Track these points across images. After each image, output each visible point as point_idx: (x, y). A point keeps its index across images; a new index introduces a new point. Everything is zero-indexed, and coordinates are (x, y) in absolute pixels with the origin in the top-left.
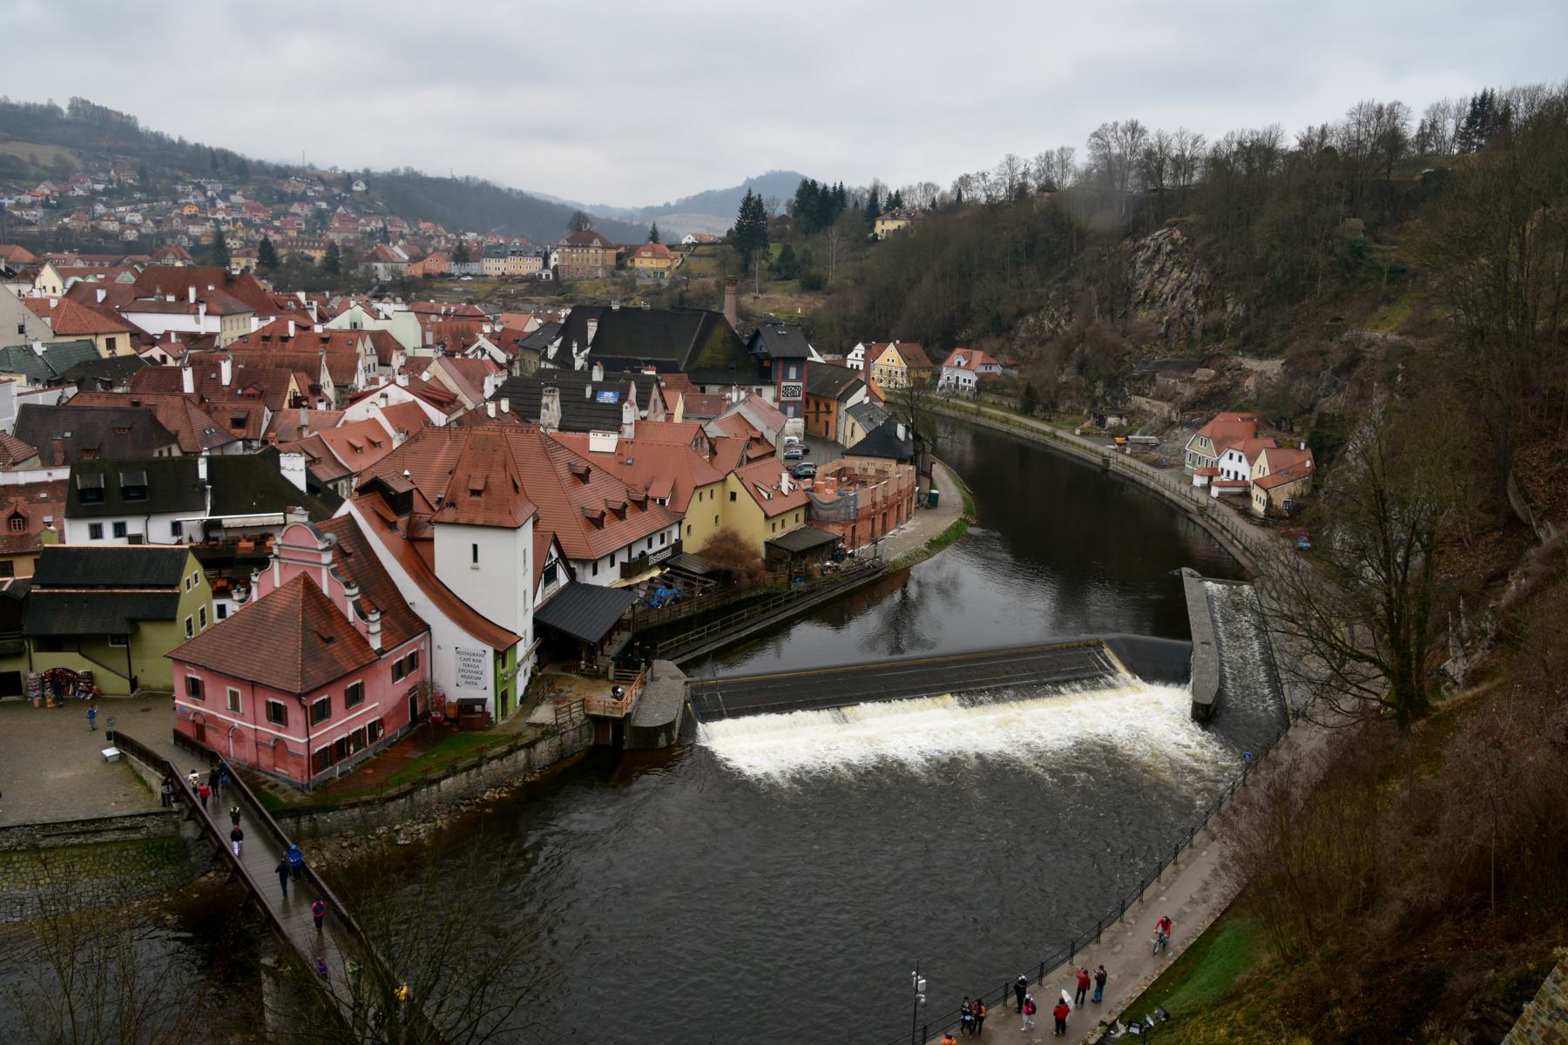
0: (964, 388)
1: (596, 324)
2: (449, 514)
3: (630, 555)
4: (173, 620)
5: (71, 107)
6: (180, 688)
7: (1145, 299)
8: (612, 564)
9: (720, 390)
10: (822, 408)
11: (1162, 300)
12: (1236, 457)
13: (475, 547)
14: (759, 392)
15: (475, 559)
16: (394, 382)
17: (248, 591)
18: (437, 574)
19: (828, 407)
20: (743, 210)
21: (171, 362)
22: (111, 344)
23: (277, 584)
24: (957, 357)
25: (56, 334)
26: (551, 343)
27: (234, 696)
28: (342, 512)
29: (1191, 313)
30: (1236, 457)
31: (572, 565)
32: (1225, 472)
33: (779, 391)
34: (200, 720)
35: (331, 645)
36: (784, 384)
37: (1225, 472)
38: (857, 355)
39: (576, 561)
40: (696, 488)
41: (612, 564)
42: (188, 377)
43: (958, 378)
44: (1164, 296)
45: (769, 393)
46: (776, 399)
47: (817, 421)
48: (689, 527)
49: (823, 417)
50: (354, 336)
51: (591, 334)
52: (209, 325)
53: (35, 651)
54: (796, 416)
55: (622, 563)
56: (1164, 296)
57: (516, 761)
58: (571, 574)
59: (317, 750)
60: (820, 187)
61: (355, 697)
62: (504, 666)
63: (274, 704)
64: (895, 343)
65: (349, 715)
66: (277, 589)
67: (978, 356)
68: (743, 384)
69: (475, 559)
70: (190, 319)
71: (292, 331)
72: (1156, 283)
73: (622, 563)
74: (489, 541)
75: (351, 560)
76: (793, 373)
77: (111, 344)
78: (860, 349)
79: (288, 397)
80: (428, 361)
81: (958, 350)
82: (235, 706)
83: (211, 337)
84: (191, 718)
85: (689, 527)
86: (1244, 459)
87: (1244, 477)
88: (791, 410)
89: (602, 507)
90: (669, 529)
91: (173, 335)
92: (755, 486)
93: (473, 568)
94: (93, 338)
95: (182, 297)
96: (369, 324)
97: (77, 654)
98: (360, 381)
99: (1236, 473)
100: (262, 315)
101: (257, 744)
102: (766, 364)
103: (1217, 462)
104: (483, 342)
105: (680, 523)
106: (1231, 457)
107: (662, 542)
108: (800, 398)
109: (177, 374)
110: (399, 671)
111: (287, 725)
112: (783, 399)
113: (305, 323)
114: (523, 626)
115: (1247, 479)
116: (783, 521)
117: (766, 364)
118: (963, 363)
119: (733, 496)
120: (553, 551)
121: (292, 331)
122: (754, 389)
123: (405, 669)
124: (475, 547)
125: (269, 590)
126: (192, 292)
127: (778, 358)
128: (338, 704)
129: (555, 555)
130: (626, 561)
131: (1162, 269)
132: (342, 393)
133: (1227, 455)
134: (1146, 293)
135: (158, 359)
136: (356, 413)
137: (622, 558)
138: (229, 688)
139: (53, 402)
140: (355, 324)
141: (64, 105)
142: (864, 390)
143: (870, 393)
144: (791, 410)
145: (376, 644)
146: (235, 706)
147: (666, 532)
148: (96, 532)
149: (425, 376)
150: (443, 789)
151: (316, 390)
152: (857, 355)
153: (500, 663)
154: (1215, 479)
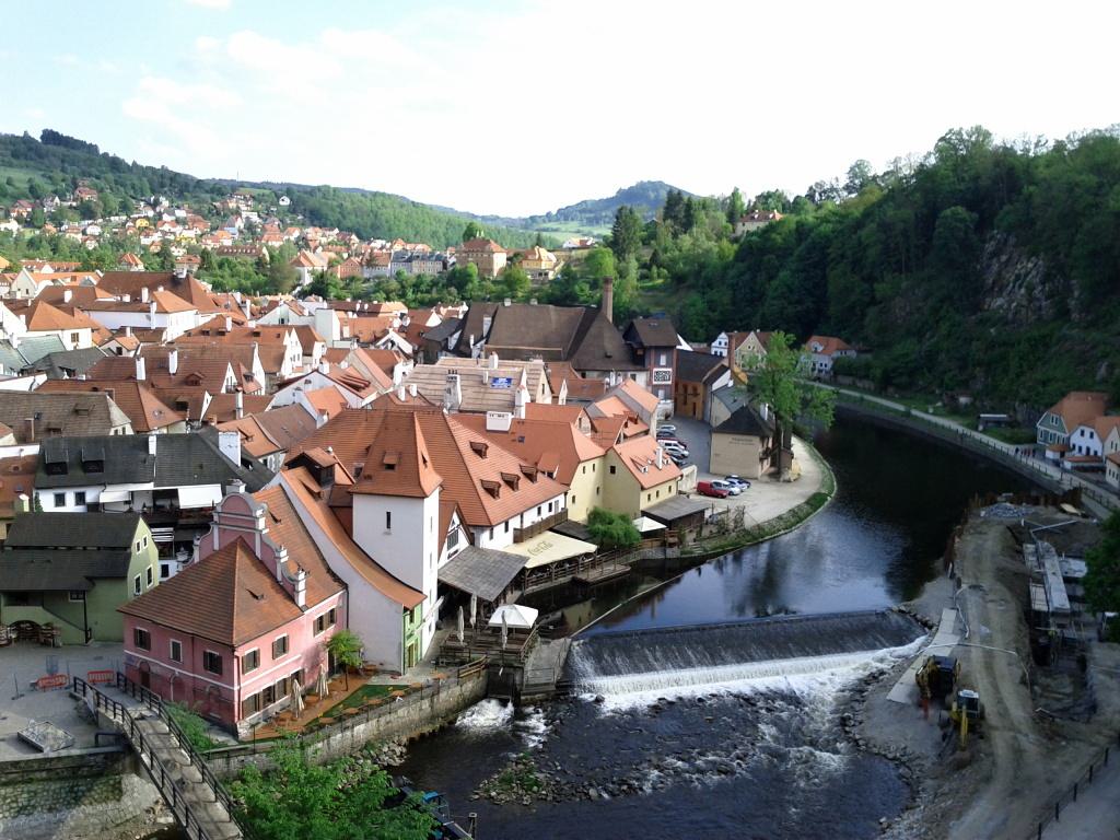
0: (820, 371)
1: (490, 319)
2: (367, 486)
3: (522, 522)
4: (124, 578)
5: (42, 137)
6: (129, 638)
7: (992, 288)
8: (507, 530)
9: (599, 376)
10: (690, 390)
12: (1087, 434)
13: (389, 514)
14: (634, 377)
15: (389, 526)
16: (317, 370)
17: (191, 552)
18: (354, 539)
19: (695, 389)
21: (125, 354)
22: (75, 338)
23: (216, 547)
24: (815, 343)
25: (28, 330)
26: (451, 335)
27: (176, 646)
28: (274, 482)
29: (1038, 299)
30: (1087, 434)
31: (472, 531)
32: (1077, 448)
34: (145, 669)
35: (262, 602)
36: (655, 370)
37: (1077, 448)
38: (720, 343)
39: (475, 526)
40: (580, 462)
41: (507, 530)
42: (141, 366)
45: (642, 378)
46: (649, 383)
47: (685, 403)
48: (574, 498)
49: (691, 399)
50: (280, 330)
51: (486, 328)
52: (155, 322)
53: (6, 605)
54: (666, 399)
55: (515, 529)
57: (421, 710)
58: (472, 540)
59: (246, 698)
60: (685, 198)
61: (282, 647)
62: (412, 621)
63: (211, 654)
64: (755, 331)
65: (278, 663)
66: (216, 553)
67: (834, 341)
68: (619, 371)
69: (389, 526)
70: (144, 315)
71: (229, 326)
73: (515, 529)
74: (399, 508)
75: (279, 525)
76: (663, 360)
77: (75, 338)
78: (723, 337)
79: (225, 383)
80: (347, 351)
81: (815, 338)
82: (177, 656)
83: (160, 331)
84: (138, 665)
85: (574, 498)
86: (1095, 436)
88: (661, 393)
89: (497, 478)
90: (556, 499)
91: (128, 330)
92: (633, 461)
93: (389, 534)
94: (59, 332)
95: (136, 298)
96: (294, 320)
97: (41, 608)
98: (287, 371)
99: (1088, 449)
100: (203, 311)
101: (194, 691)
102: (640, 352)
103: (1069, 439)
104: (393, 335)
105: (566, 494)
106: (1082, 433)
107: (550, 510)
108: (670, 383)
109: (132, 363)
110: (320, 625)
111: (221, 674)
112: (655, 383)
113: (239, 318)
114: (430, 586)
115: (1099, 454)
116: (658, 493)
117: (640, 352)
119: (613, 470)
120: (455, 517)
121: (229, 326)
122: (629, 374)
123: (325, 624)
124: (389, 514)
125: (207, 553)
126: (145, 292)
127: (651, 347)
128: (265, 657)
129: (457, 521)
130: (519, 527)
132: (271, 379)
133: (1079, 432)
134: (994, 283)
135: (115, 350)
136: (283, 397)
137: (515, 523)
138: (172, 640)
139: (26, 389)
140: (283, 320)
141: (37, 135)
142: (728, 373)
143: (734, 376)
144: (661, 393)
145: (301, 600)
146: (177, 656)
147: (553, 501)
148: (60, 500)
149: (344, 365)
150: (355, 733)
151: (249, 378)
152: (720, 343)
153: (408, 618)
154: (1067, 454)
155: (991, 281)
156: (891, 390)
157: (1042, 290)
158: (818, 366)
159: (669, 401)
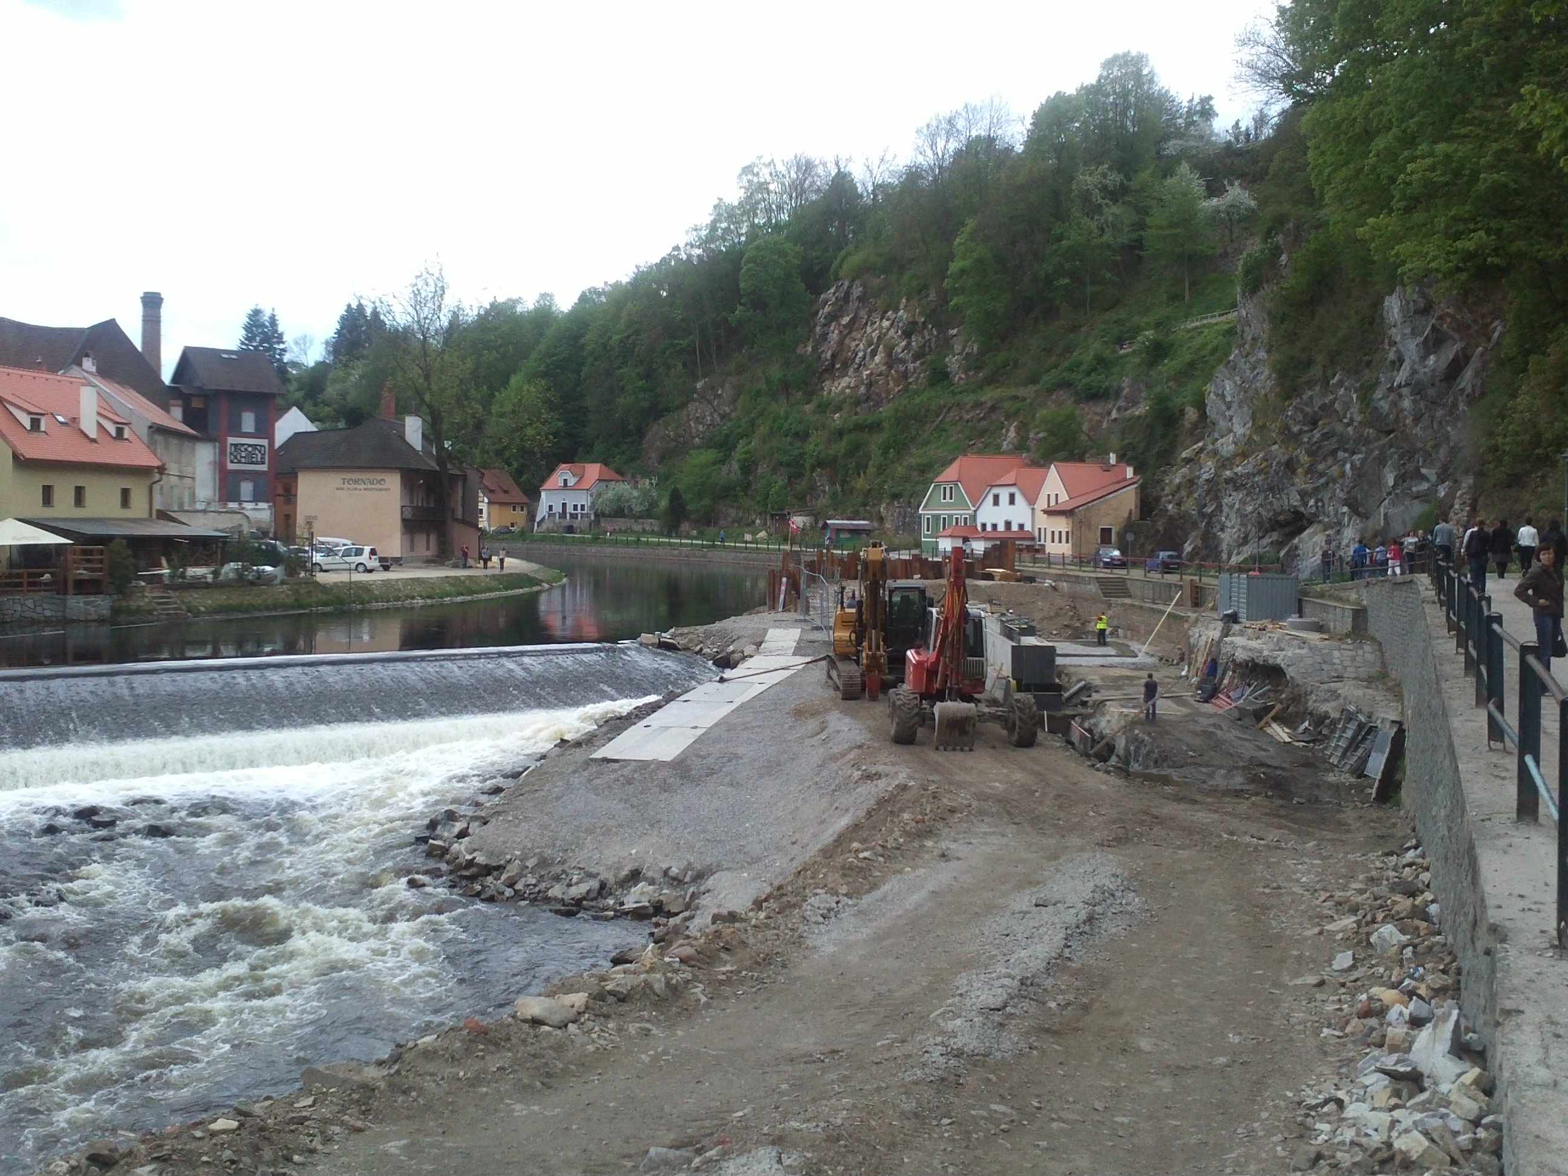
7: (833, 364)
11: (857, 360)
12: (1004, 498)
20: (248, 328)
29: (903, 361)
30: (1004, 498)
33: (222, 452)
36: (231, 440)
43: (564, 505)
44: (860, 354)
54: (256, 499)
56: (860, 354)
67: (593, 470)
72: (847, 341)
86: (1018, 497)
87: (1021, 526)
88: (246, 488)
99: (1008, 524)
103: (974, 517)
106: (996, 498)
108: (264, 468)
112: (231, 466)
115: (1028, 528)
118: (571, 482)
127: (218, 394)
131: (853, 321)
133: (990, 499)
134: (833, 356)
144: (246, 488)
155: (829, 356)
156: (685, 526)
157: (908, 347)
158: (570, 509)
159: (263, 505)
